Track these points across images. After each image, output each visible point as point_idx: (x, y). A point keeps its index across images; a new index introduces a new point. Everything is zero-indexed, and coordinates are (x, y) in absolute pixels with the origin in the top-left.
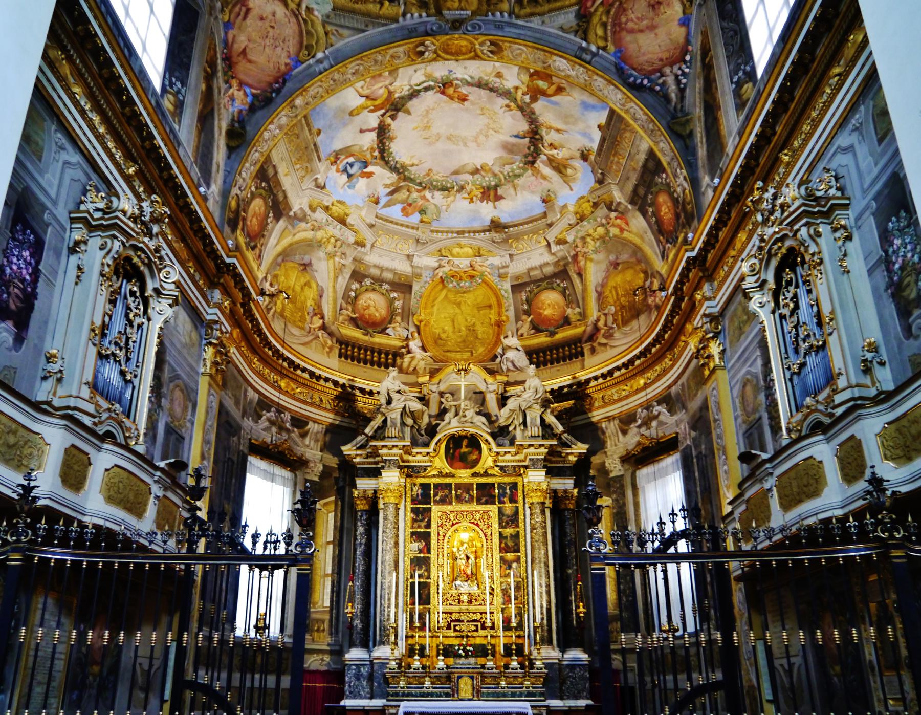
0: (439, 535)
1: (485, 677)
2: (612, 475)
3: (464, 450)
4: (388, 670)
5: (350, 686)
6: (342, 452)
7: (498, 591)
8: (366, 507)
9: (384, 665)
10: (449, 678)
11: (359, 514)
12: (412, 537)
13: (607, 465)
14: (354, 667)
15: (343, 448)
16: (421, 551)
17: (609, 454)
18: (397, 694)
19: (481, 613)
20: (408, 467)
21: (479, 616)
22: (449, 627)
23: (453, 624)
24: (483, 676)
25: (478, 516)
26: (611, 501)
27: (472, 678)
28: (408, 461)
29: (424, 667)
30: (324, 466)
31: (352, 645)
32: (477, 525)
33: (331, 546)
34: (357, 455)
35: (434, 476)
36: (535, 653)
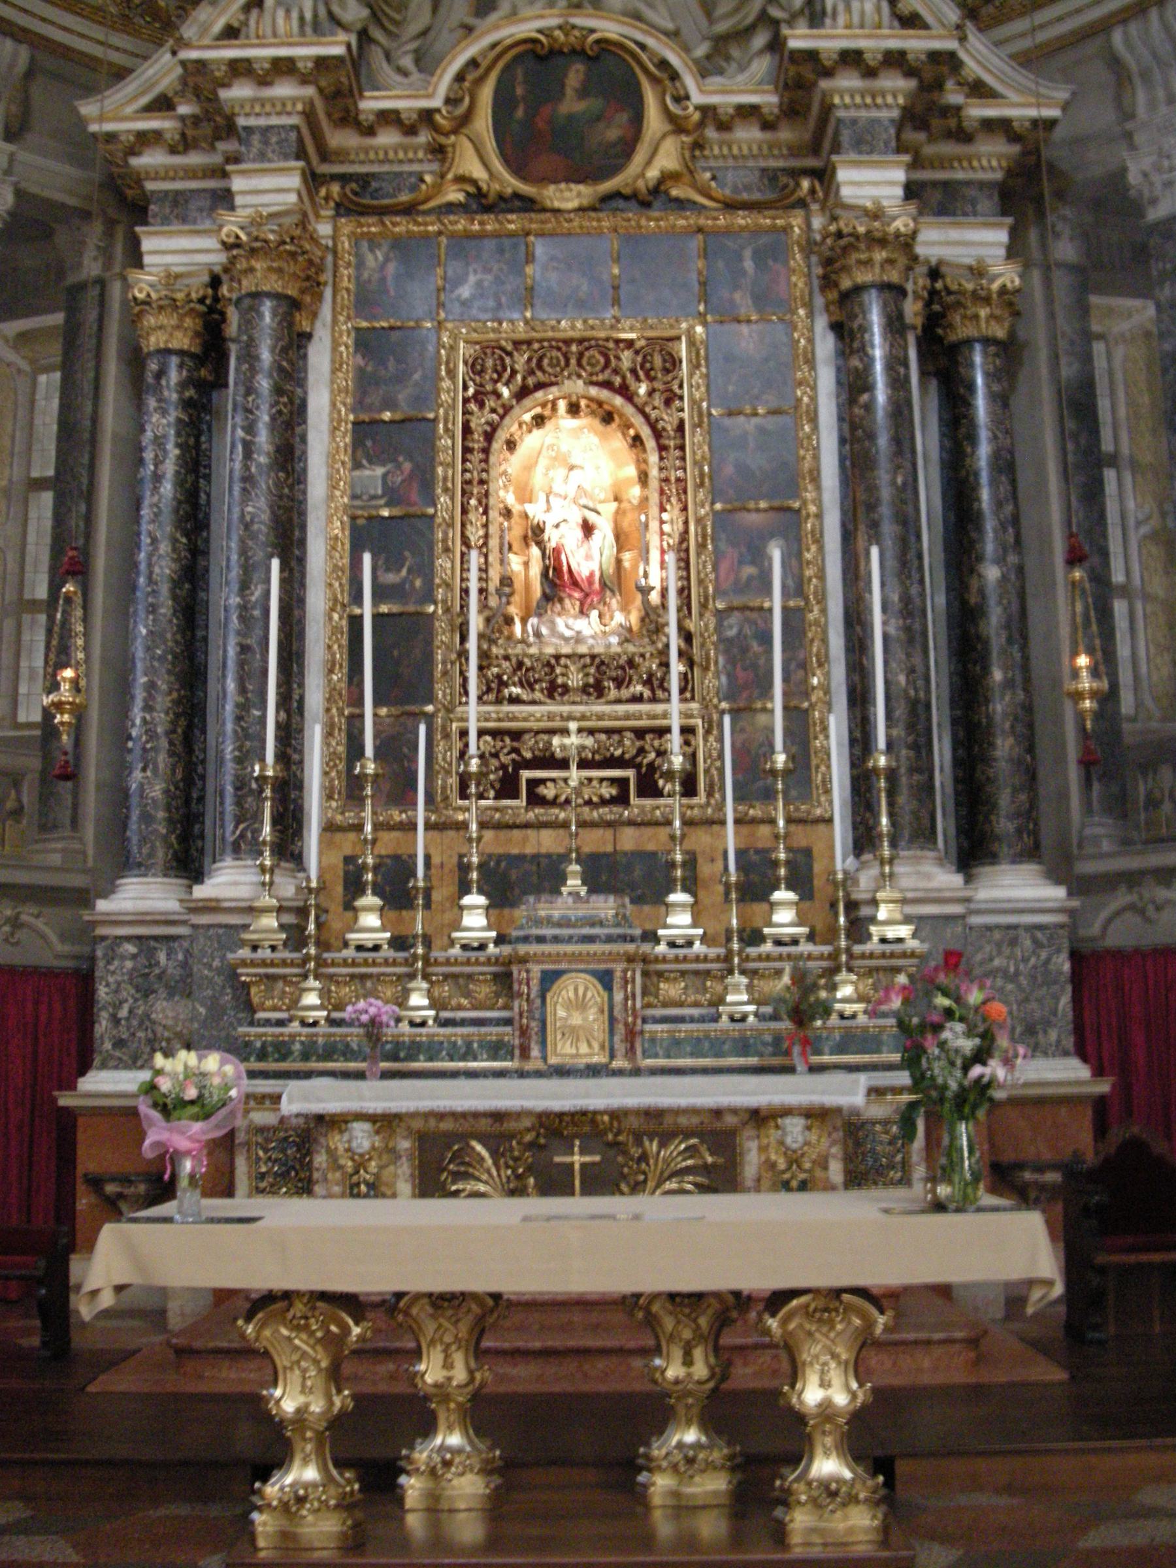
0: (467, 430)
1: (660, 974)
2: (1154, 214)
3: (571, 105)
4: (244, 953)
5: (115, 1020)
6: (82, 122)
7: (708, 648)
8: (182, 341)
9: (232, 935)
10: (504, 979)
11: (153, 366)
12: (358, 443)
13: (1133, 178)
14: (131, 948)
15: (88, 109)
16: (392, 496)
17: (1139, 138)
18: (282, 1050)
19: (640, 733)
20: (344, 178)
21: (629, 745)
22: (508, 788)
23: (526, 774)
24: (653, 972)
25: (626, 359)
26: (1151, 311)
27: (605, 979)
28: (341, 155)
29: (400, 942)
30: (19, 193)
31: (141, 868)
32: (625, 392)
33: (47, 497)
34: (145, 140)
35: (451, 208)
36: (866, 880)
